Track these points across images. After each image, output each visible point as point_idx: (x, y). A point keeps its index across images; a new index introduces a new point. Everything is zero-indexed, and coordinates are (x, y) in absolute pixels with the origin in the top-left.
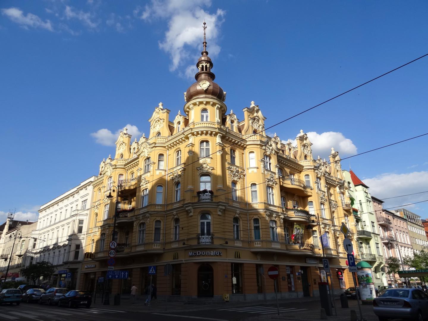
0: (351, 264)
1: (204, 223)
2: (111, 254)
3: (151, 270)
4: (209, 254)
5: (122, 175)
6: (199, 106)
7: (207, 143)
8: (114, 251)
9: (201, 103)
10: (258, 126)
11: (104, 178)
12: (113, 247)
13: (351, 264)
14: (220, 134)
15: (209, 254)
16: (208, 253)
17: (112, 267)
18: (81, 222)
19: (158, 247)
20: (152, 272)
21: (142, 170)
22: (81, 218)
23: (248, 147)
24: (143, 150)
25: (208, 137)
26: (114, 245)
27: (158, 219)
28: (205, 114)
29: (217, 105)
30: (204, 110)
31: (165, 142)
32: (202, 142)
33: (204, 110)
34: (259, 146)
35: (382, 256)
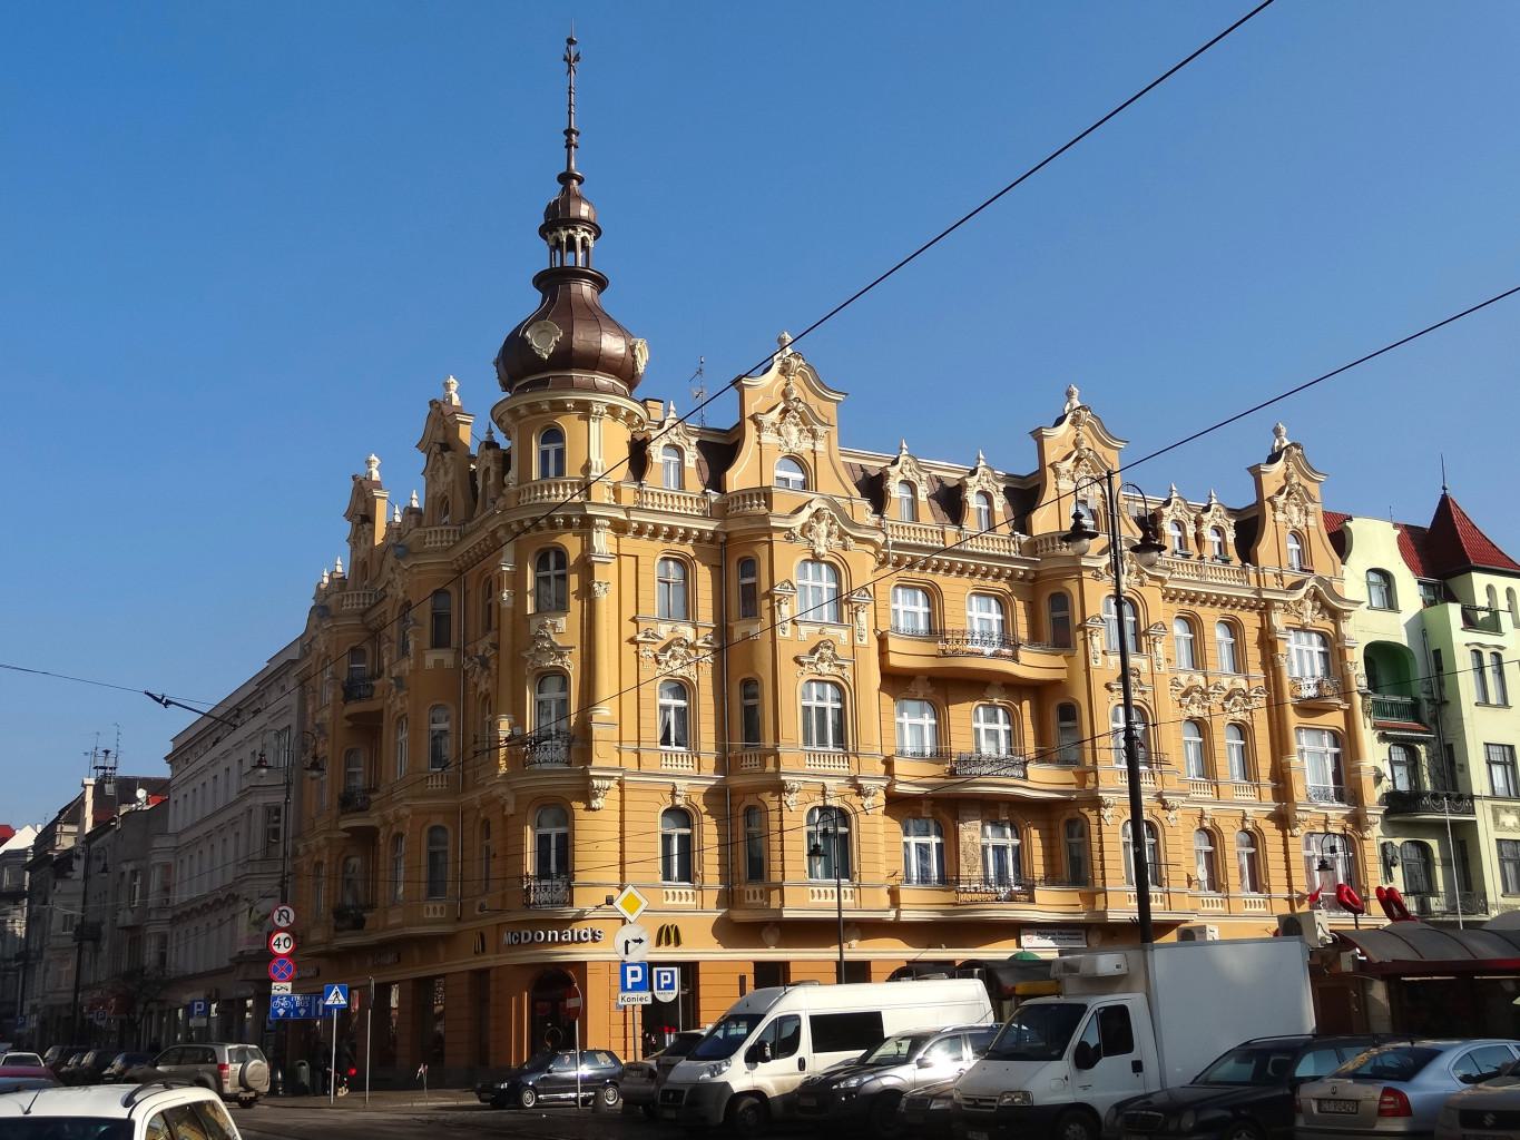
0: (629, 986)
1: (548, 837)
2: (279, 945)
3: (332, 997)
4: (557, 939)
8: (286, 935)
12: (283, 924)
13: (629, 986)
15: (557, 939)
16: (553, 935)
17: (283, 985)
19: (438, 915)
20: (337, 1003)
26: (287, 919)
27: (438, 821)
28: (552, 448)
31: (451, 544)
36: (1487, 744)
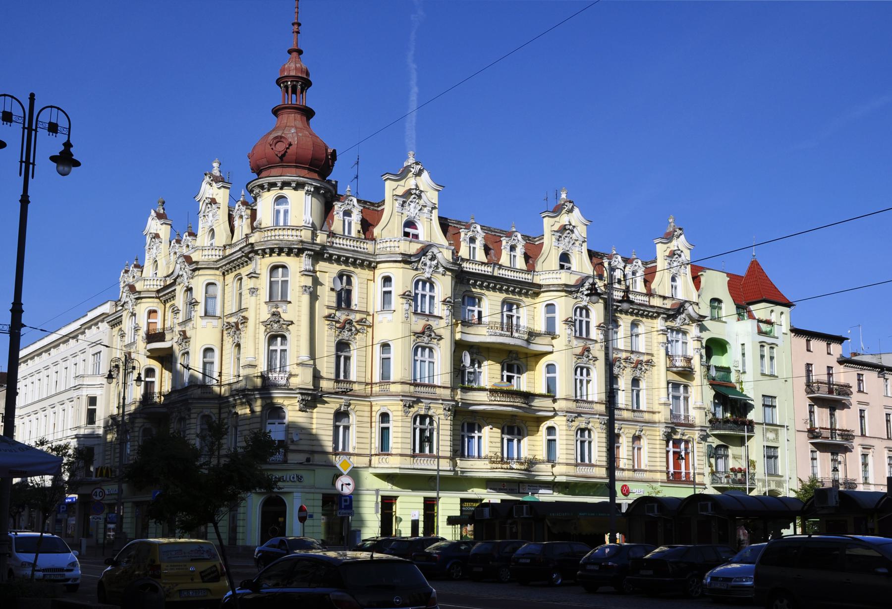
5: (155, 311)
6: (269, 190)
7: (285, 270)
9: (273, 185)
10: (420, 210)
11: (124, 314)
14: (309, 252)
18: (93, 401)
21: (181, 313)
22: (92, 392)
23: (380, 266)
24: (181, 273)
25: (283, 259)
28: (282, 208)
29: (306, 188)
30: (280, 199)
31: (218, 258)
32: (274, 268)
33: (280, 199)
34: (402, 265)
35: (782, 476)
36: (763, 396)
